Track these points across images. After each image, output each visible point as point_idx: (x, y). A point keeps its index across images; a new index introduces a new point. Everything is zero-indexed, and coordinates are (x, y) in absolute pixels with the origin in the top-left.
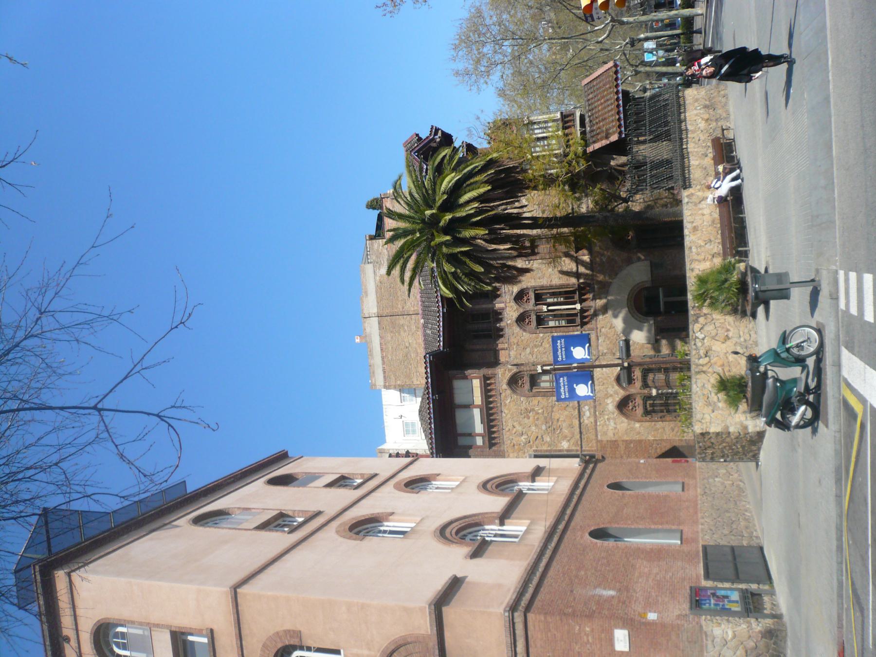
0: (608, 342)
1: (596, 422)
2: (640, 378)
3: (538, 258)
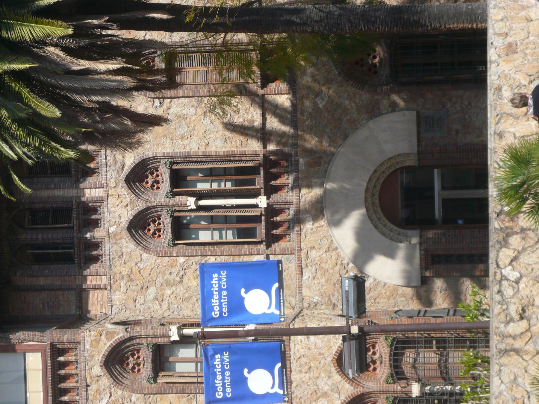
0: (323, 280)
2: (386, 358)
3: (180, 93)
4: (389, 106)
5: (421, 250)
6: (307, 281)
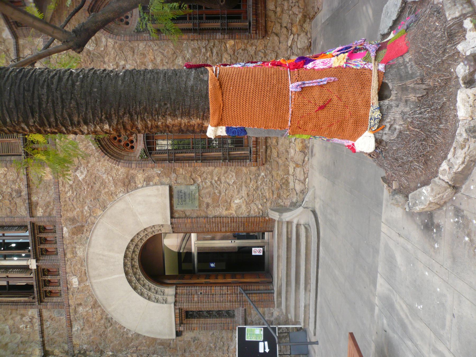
0: (90, 331)
4: (144, 181)
5: (175, 309)
6: (76, 333)
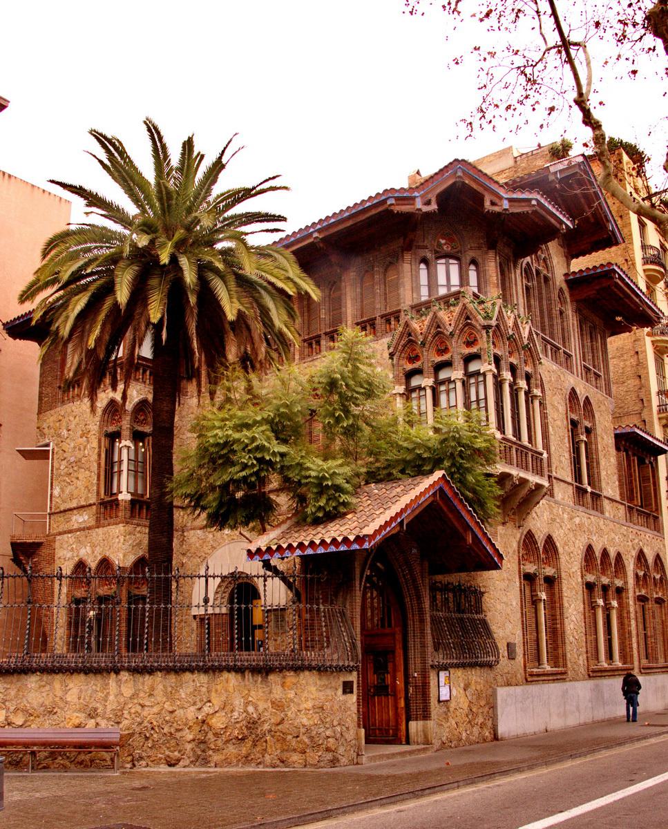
1: (70, 532)
